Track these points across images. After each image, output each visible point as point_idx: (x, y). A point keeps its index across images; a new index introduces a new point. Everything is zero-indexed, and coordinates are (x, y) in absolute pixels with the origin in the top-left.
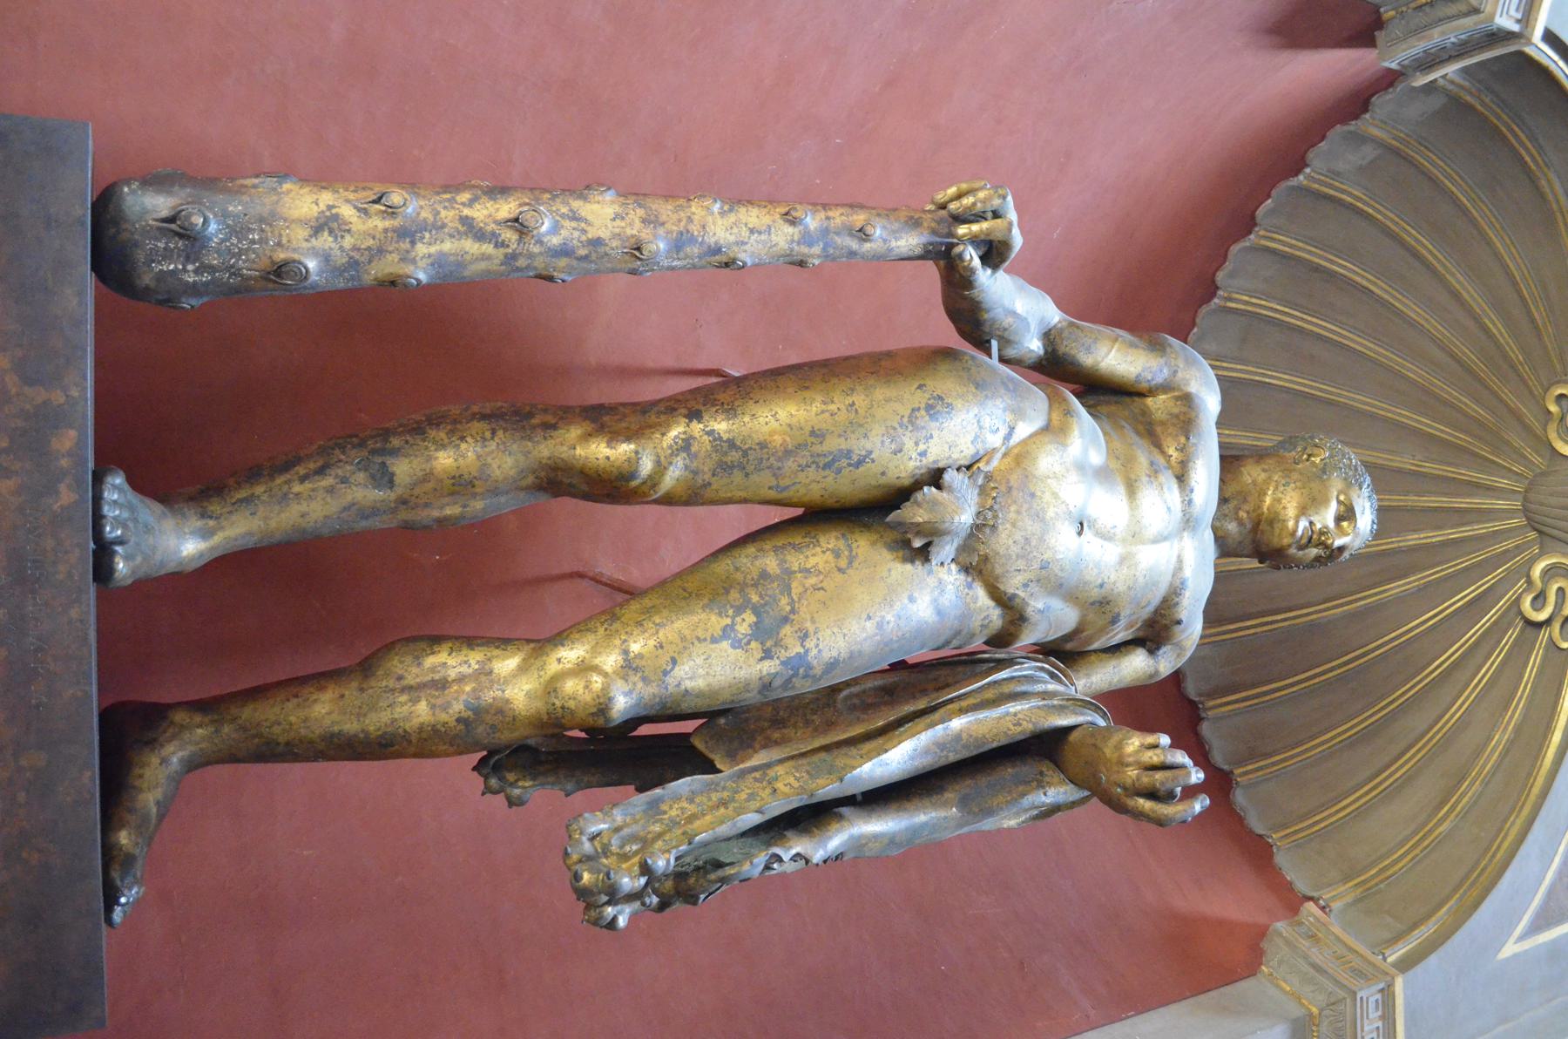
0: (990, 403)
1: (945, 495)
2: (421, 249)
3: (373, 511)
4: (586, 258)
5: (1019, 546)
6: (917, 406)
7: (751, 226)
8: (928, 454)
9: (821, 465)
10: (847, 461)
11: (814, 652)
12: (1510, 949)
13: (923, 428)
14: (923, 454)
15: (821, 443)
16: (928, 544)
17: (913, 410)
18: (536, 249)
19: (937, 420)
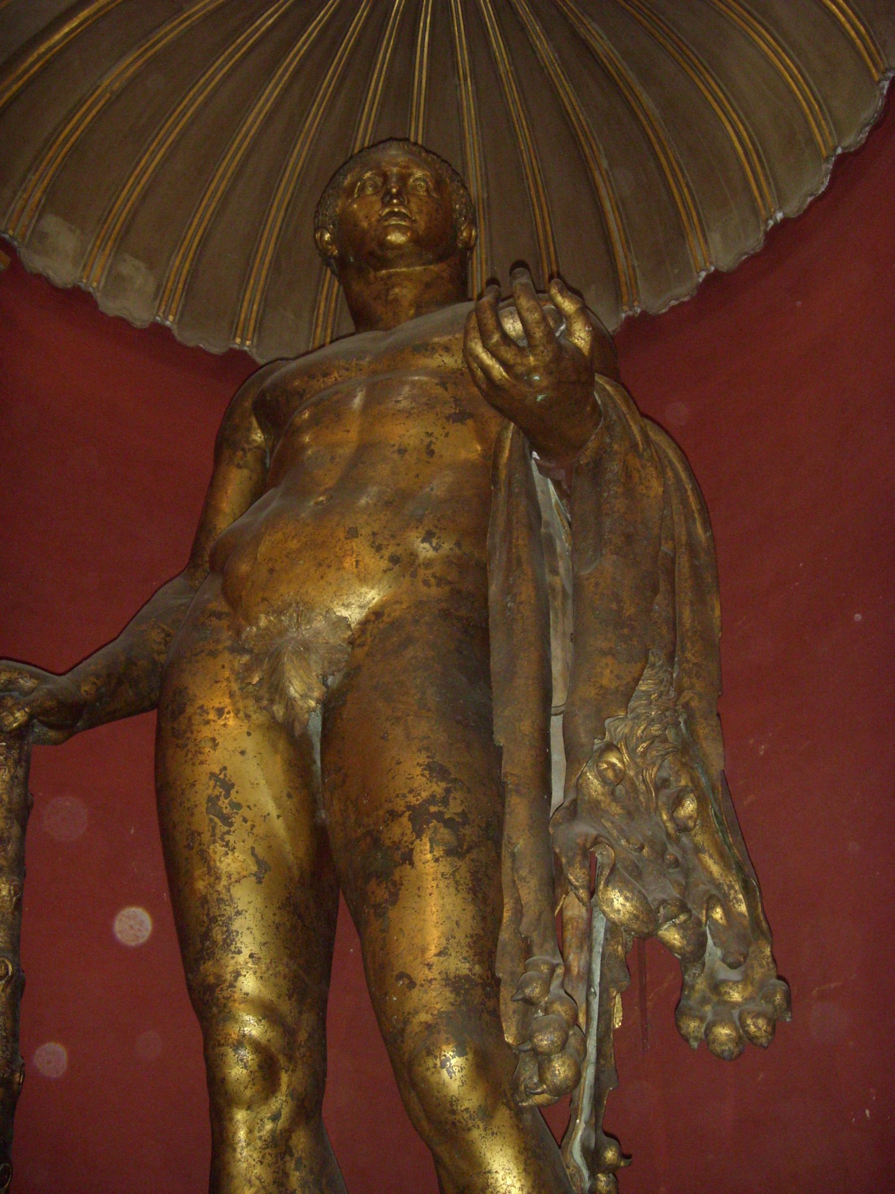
8: (222, 705)
9: (226, 829)
10: (222, 798)
13: (190, 719)
15: (199, 834)
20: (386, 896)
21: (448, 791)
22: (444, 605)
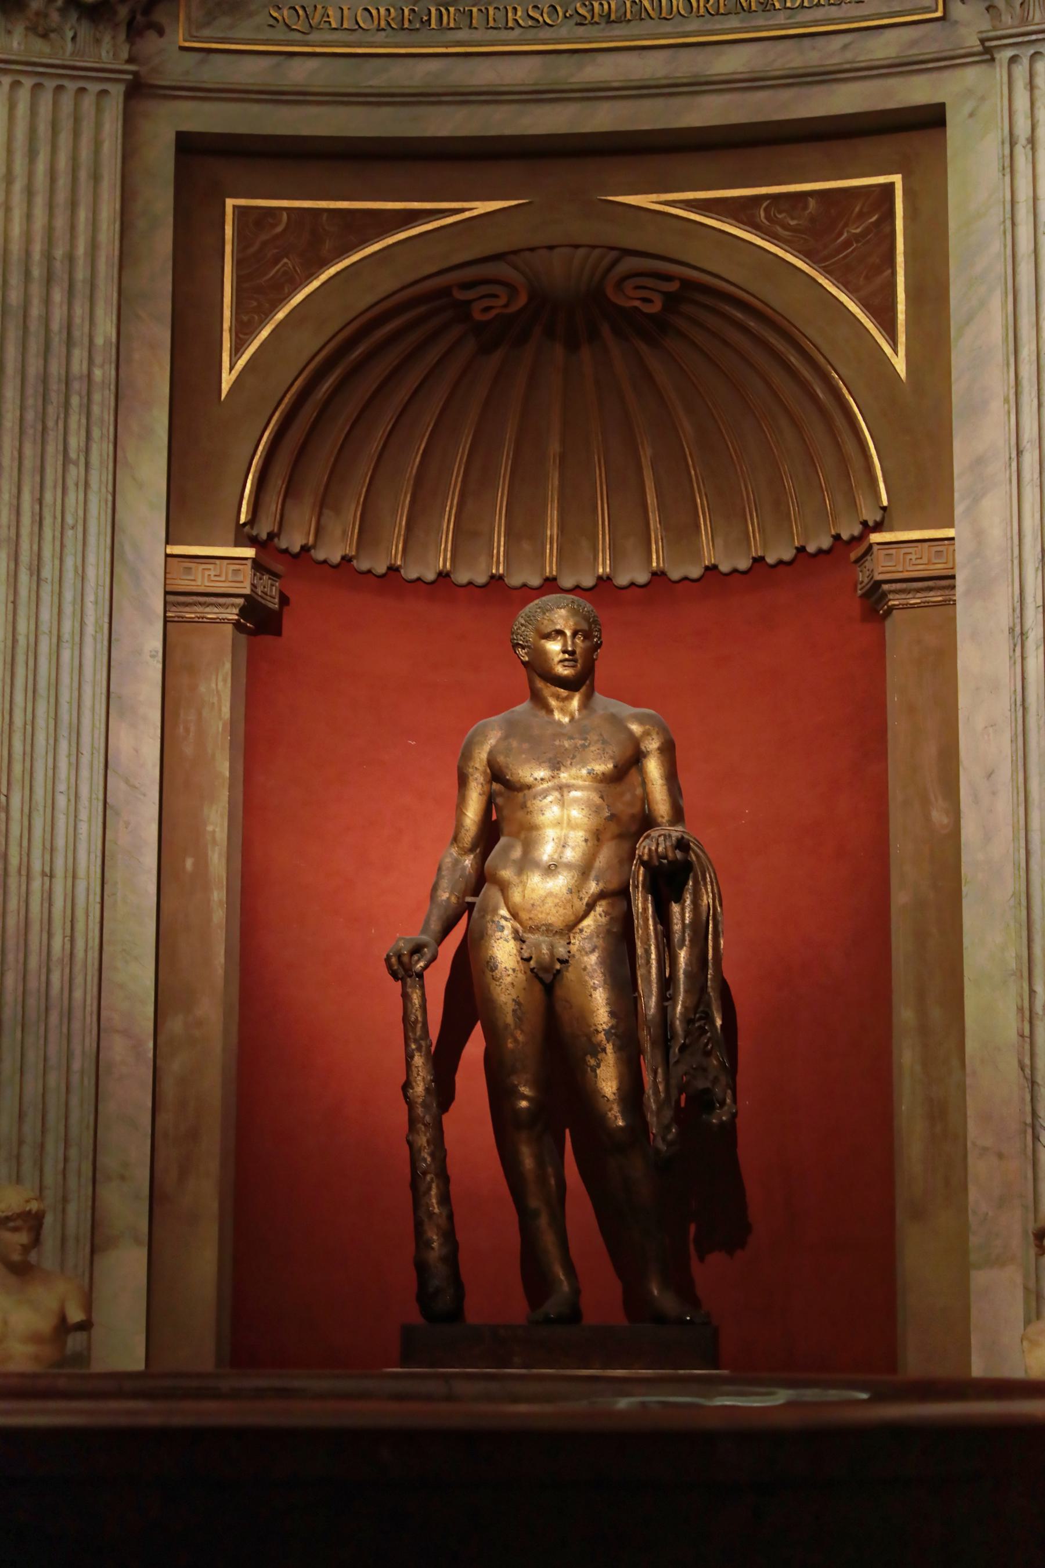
0: (490, 932)
1: (533, 956)
2: (436, 1210)
5: (559, 909)
6: (491, 977)
7: (416, 1075)
8: (514, 967)
11: (605, 1026)
12: (900, 365)
13: (501, 973)
14: (514, 970)
16: (558, 960)
17: (493, 979)
19: (497, 965)
20: (595, 1064)
21: (617, 1023)
22: (608, 927)
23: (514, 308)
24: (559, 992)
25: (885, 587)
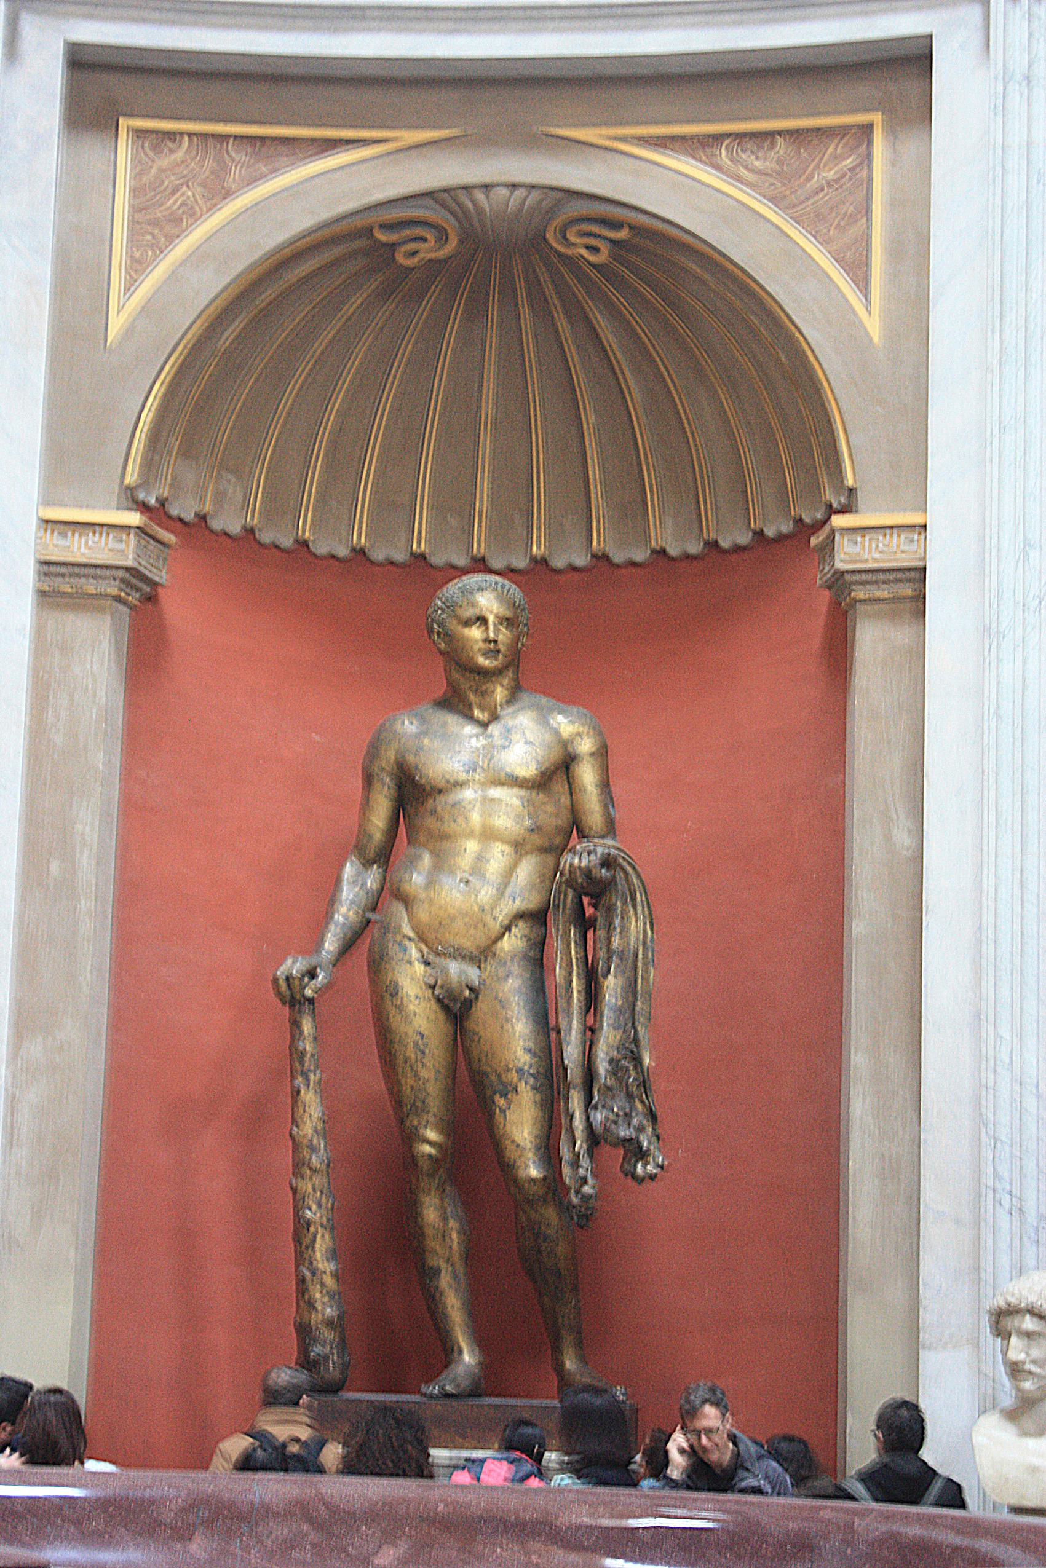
3: (455, 1276)
4: (322, 1192)
18: (318, 1215)
23: (442, 254)
24: (471, 1025)
25: (847, 577)
